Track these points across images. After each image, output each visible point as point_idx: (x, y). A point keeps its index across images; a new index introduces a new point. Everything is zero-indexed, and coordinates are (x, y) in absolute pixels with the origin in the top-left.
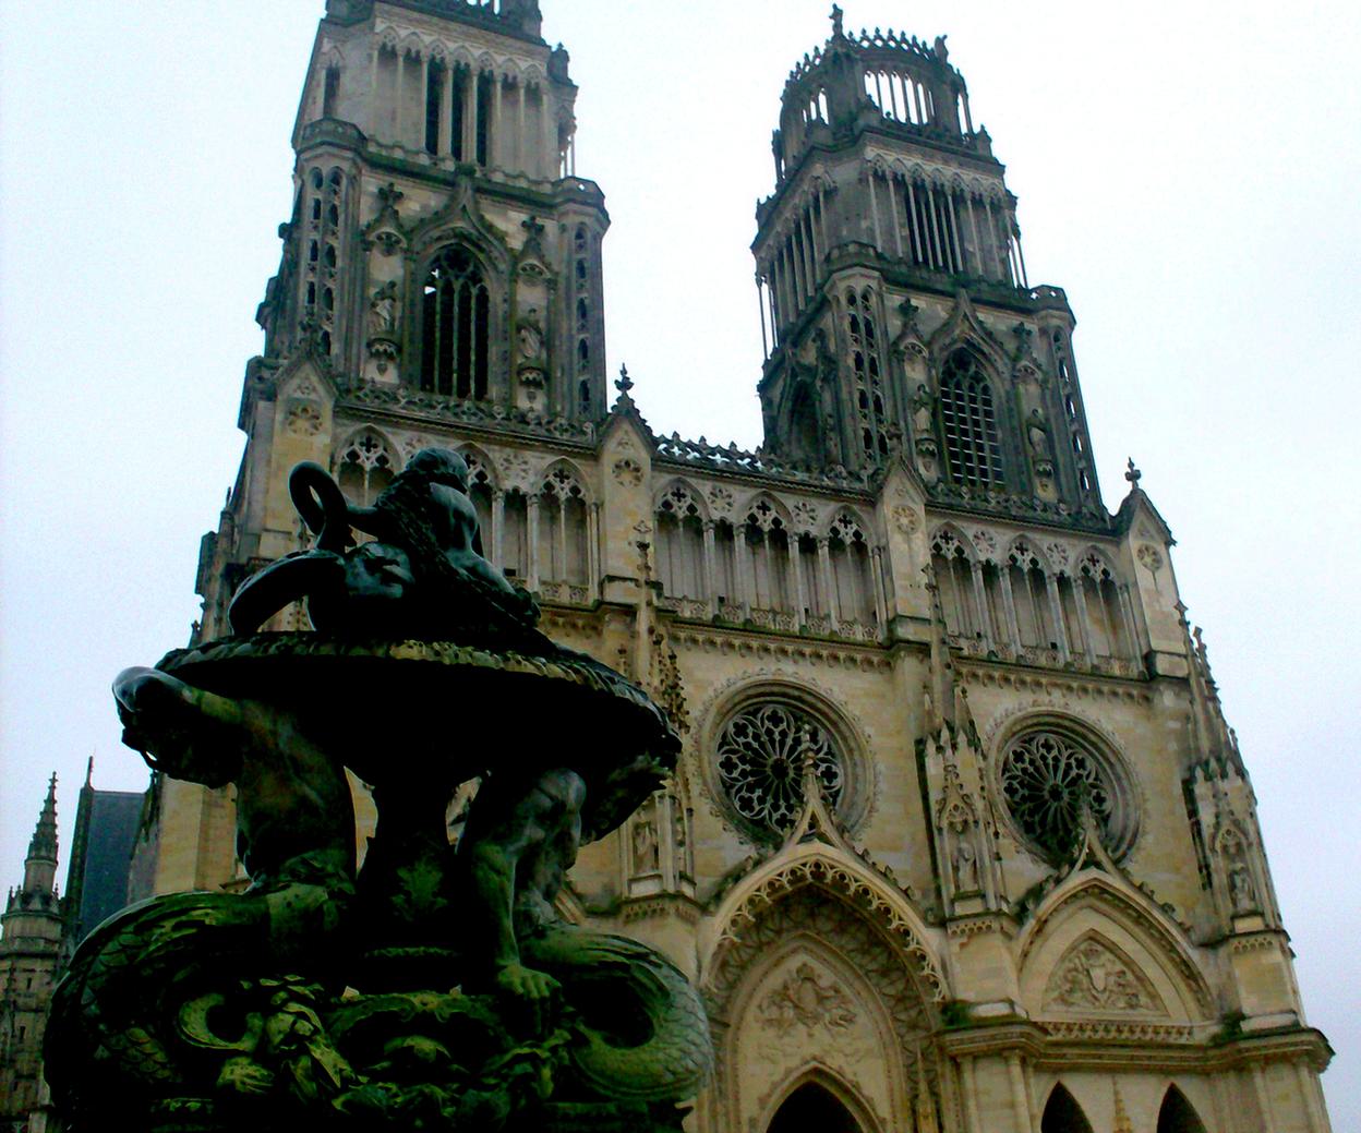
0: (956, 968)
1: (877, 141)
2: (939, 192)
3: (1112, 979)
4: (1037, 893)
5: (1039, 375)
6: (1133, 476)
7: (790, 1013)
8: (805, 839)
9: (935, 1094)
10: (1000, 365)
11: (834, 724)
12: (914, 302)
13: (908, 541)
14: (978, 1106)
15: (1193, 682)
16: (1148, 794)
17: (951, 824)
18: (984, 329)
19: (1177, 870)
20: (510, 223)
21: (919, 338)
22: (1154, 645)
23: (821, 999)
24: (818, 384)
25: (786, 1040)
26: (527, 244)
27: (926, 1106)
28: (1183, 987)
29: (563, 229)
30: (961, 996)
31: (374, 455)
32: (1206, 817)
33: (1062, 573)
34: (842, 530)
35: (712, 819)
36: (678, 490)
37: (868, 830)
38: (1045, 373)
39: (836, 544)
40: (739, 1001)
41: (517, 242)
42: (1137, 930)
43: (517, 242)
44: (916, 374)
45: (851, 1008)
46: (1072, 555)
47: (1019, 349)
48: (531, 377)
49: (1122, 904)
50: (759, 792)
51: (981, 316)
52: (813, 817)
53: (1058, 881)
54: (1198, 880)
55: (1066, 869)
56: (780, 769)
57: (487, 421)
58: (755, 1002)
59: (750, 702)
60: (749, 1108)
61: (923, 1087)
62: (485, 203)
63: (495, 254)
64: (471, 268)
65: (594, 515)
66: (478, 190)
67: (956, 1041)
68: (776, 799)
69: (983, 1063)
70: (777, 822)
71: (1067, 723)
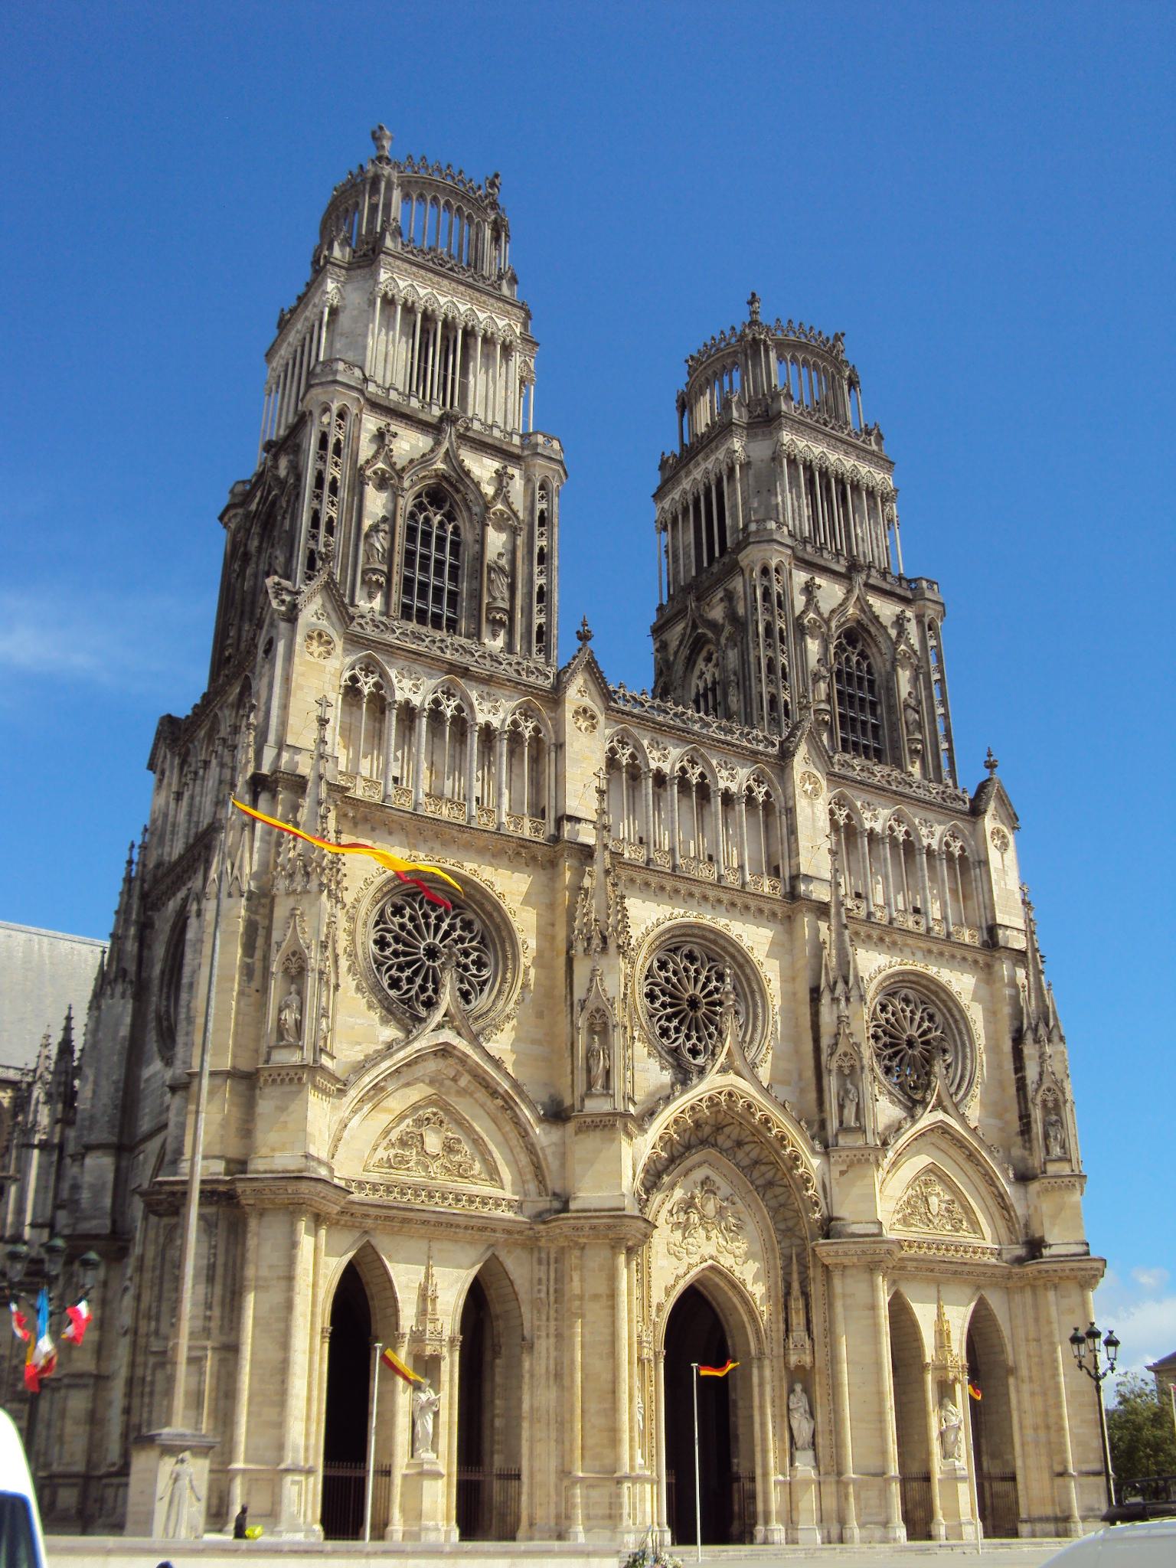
0: (835, 1191)
1: (792, 428)
2: (841, 482)
3: (943, 1206)
4: (897, 1129)
5: (914, 661)
6: (991, 766)
7: (695, 1217)
8: (723, 1070)
9: (806, 1295)
10: (883, 646)
11: (741, 966)
12: (818, 581)
13: (812, 806)
14: (845, 1307)
15: (1030, 955)
17: (840, 1067)
20: (482, 468)
22: (999, 921)
24: (723, 641)
25: (690, 1240)
27: (797, 1304)
28: (997, 1215)
29: (528, 480)
30: (835, 1215)
32: (1031, 1073)
39: (750, 800)
41: (489, 490)
42: (968, 1167)
43: (489, 490)
44: (813, 646)
46: (939, 829)
48: (498, 617)
49: (959, 1143)
50: (675, 1022)
51: (872, 599)
54: (1016, 1126)
56: (693, 1003)
57: (468, 657)
60: (657, 1296)
61: (796, 1285)
63: (471, 497)
64: (447, 507)
65: (553, 755)
68: (689, 1029)
69: (848, 1272)
70: (690, 1051)
71: (924, 982)
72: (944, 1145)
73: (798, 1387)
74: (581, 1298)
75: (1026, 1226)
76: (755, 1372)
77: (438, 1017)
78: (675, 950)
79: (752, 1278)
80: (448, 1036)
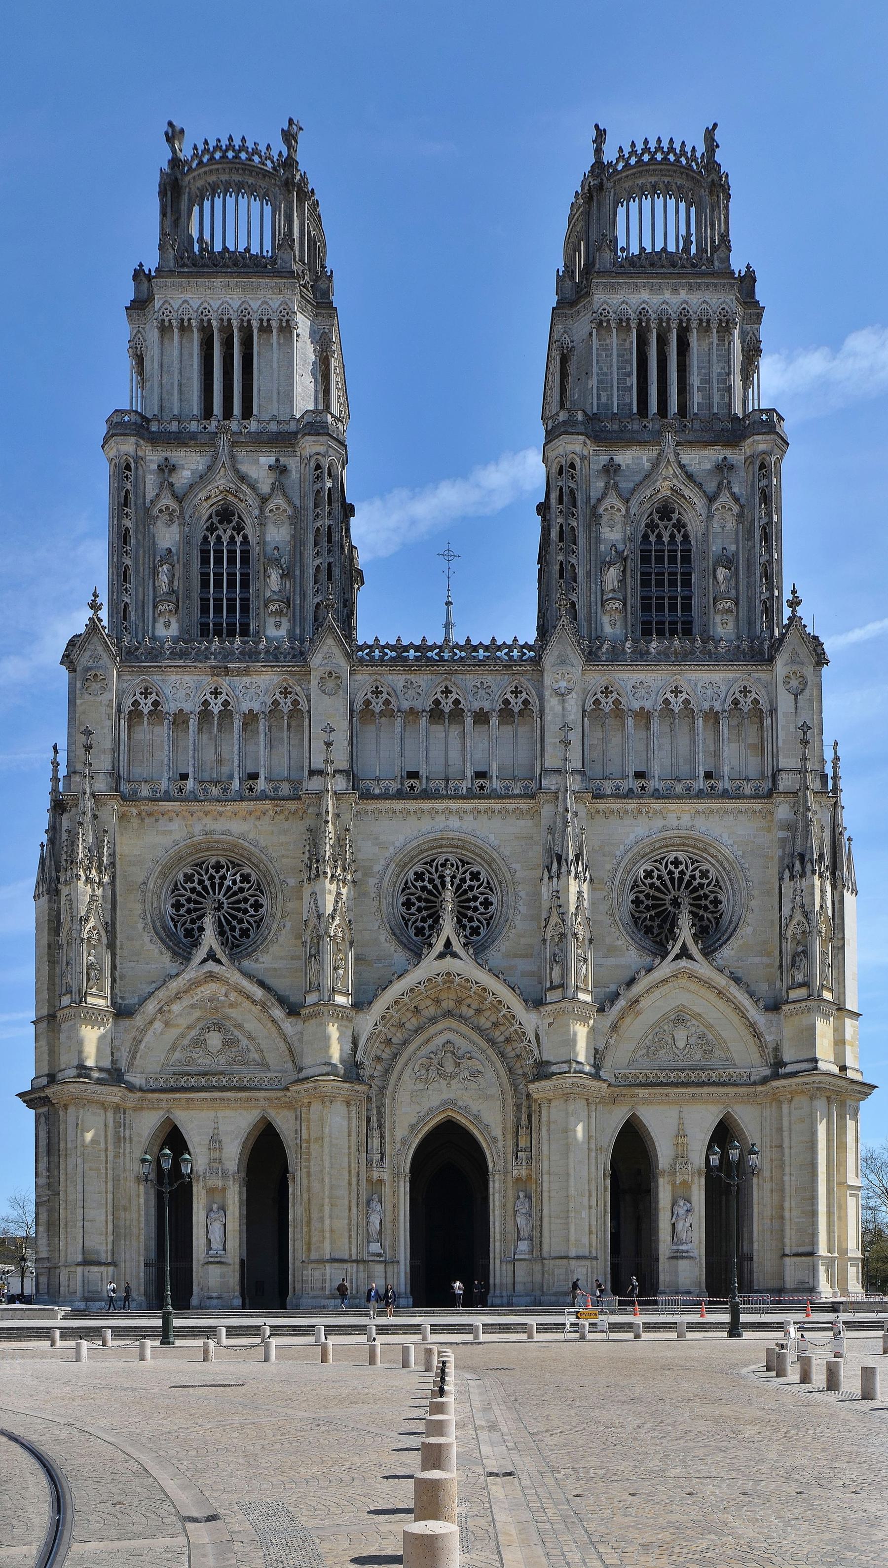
5: (736, 509)
7: (433, 1074)
11: (490, 865)
14: (548, 1130)
16: (755, 892)
18: (686, 473)
19: (769, 954)
21: (620, 495)
23: (457, 1065)
26: (273, 487)
31: (149, 701)
33: (711, 709)
34: (512, 701)
35: (387, 945)
36: (377, 688)
37: (507, 943)
38: (742, 506)
40: (399, 1067)
41: (265, 489)
42: (721, 1004)
43: (265, 489)
45: (480, 1068)
47: (720, 484)
52: (448, 940)
53: (650, 970)
55: (657, 961)
58: (410, 1066)
59: (426, 854)
61: (524, 1117)
62: (241, 454)
66: (234, 444)
67: (538, 1089)
69: (553, 1104)
71: (691, 842)
72: (693, 986)
73: (522, 1195)
74: (308, 1141)
75: (777, 1049)
76: (491, 1184)
77: (201, 953)
78: (430, 863)
79: (487, 1116)
80: (211, 965)
